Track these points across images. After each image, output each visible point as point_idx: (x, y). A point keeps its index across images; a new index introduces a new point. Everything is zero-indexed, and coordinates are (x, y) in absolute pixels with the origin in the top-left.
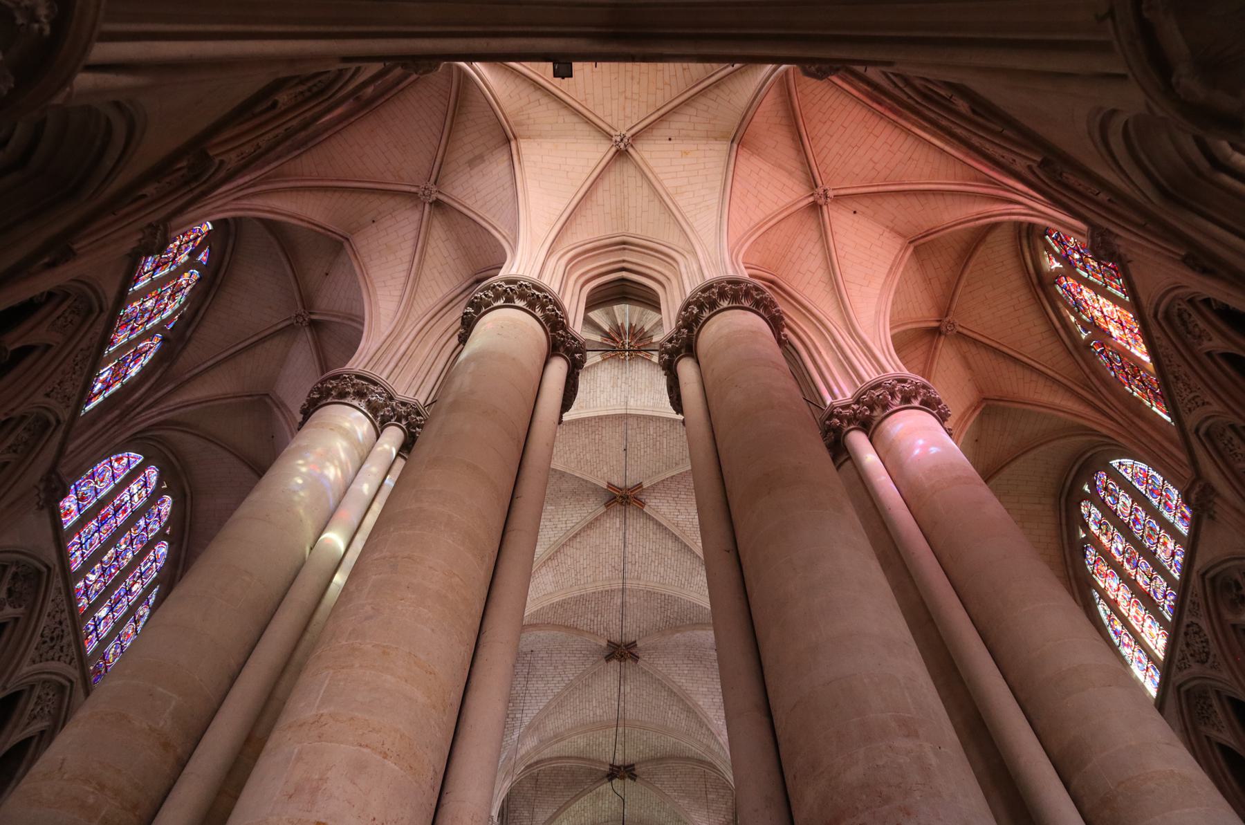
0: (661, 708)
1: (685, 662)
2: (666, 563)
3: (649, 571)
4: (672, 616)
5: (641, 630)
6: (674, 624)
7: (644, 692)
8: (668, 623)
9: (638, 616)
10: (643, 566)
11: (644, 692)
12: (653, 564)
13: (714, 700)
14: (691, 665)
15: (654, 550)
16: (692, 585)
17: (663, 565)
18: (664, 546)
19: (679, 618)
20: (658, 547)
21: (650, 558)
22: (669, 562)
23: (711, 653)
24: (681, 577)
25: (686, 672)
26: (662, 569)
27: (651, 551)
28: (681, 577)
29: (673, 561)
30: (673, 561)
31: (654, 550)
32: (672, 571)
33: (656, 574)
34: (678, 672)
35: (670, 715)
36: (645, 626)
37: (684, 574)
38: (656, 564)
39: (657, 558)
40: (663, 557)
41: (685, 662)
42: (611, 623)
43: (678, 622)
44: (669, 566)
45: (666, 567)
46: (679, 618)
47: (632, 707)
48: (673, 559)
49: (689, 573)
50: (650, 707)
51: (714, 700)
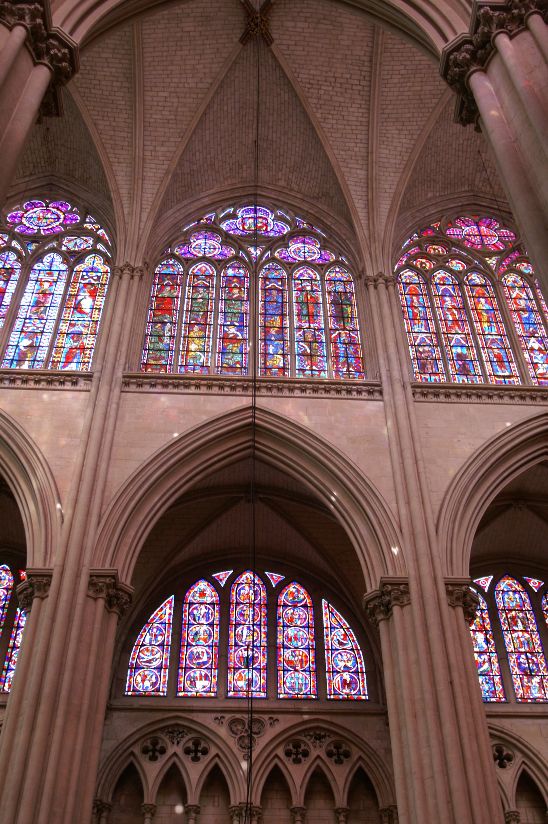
0: (169, 80)
1: (237, 105)
2: (404, 85)
3: (393, 63)
4: (322, 92)
5: (291, 48)
6: (309, 95)
7: (187, 52)
8: (308, 86)
9: (316, 45)
10: (400, 54)
11: (187, 52)
12: (402, 67)
13: (197, 153)
14: (233, 113)
15: (419, 67)
16: (384, 124)
17: (402, 80)
18: (424, 80)
19: (321, 102)
20: (423, 71)
21: (409, 63)
22: (406, 89)
23: (250, 135)
24: (392, 107)
25: (225, 108)
26: (396, 81)
27: (418, 62)
28: (392, 107)
29: (407, 93)
30: (407, 93)
31: (419, 67)
32: (396, 94)
33: (391, 72)
34: (225, 99)
35: (161, 94)
36: (298, 53)
37: (395, 111)
38: (402, 72)
39: (410, 72)
40: (411, 80)
41: (237, 105)
42: (305, 6)
43: (315, 101)
44: (401, 89)
45: (399, 85)
46: (321, 102)
47: (160, 35)
48: (410, 93)
49: (397, 118)
50: (165, 63)
51: (197, 153)
